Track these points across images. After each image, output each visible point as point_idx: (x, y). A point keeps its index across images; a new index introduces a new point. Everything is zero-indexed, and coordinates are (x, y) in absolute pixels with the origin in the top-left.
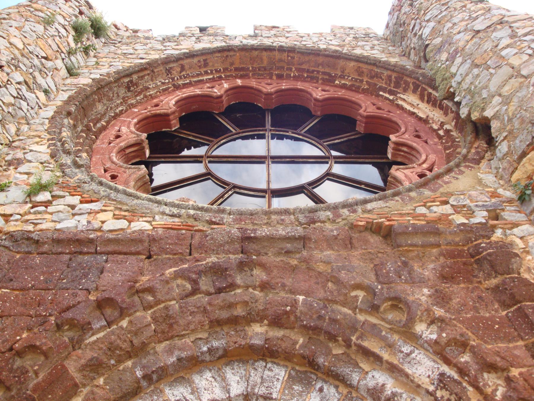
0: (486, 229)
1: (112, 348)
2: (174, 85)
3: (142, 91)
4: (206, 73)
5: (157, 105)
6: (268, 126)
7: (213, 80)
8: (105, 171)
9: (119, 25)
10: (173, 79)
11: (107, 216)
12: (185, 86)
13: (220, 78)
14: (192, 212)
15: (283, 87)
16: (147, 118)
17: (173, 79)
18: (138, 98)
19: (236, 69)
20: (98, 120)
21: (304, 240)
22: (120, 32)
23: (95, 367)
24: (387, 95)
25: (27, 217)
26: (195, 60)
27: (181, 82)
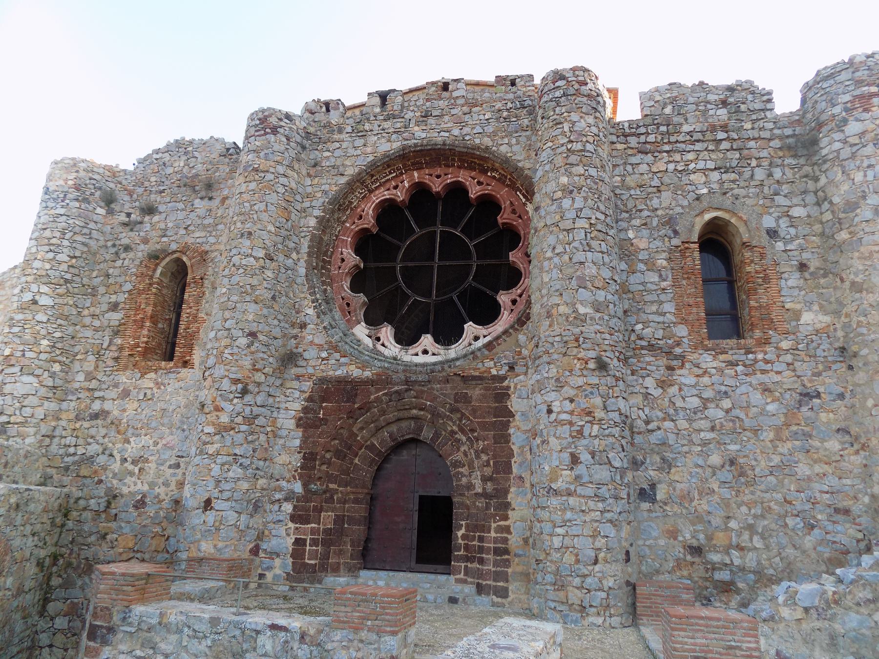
0: (503, 378)
1: (366, 423)
2: (369, 191)
3: (348, 206)
4: (390, 173)
5: (361, 217)
6: (438, 222)
7: (397, 176)
8: (343, 299)
9: (313, 106)
10: (367, 186)
11: (353, 367)
12: (376, 188)
13: (402, 174)
14: (386, 365)
15: (448, 181)
16: (357, 232)
17: (367, 186)
18: (347, 213)
19: (413, 164)
20: (328, 250)
21: (429, 381)
22: (317, 117)
23: (362, 429)
24: (521, 197)
25: (322, 367)
26: (380, 168)
27: (373, 187)
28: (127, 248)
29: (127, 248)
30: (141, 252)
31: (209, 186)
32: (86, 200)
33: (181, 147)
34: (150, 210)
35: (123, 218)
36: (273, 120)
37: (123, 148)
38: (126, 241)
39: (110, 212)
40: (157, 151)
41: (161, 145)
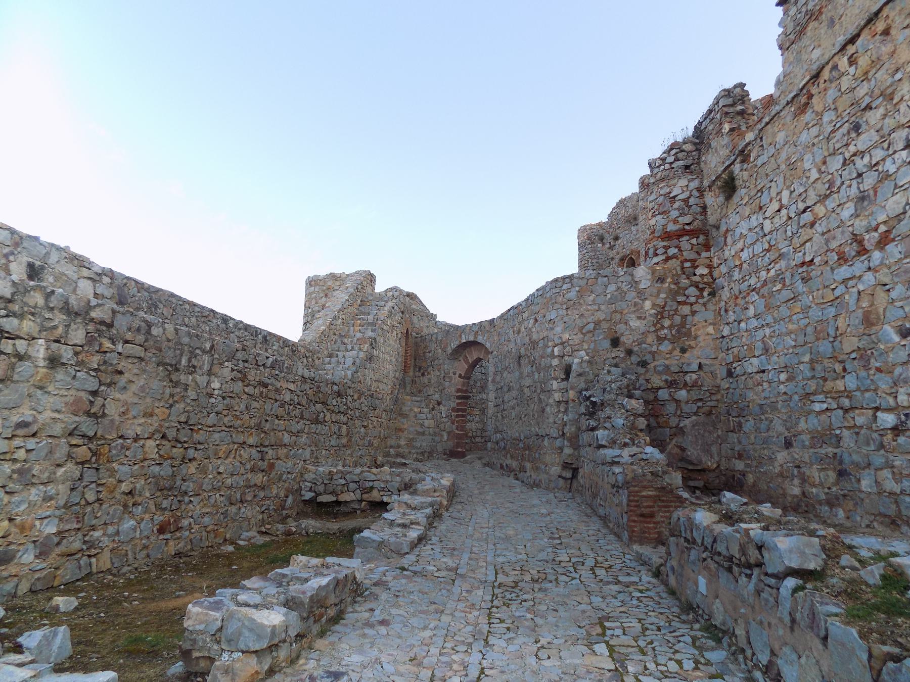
28: (612, 259)
29: (612, 259)
30: (618, 257)
31: (635, 219)
32: (593, 243)
33: (622, 203)
34: (616, 238)
35: (608, 246)
36: (646, 181)
37: (600, 214)
38: (611, 256)
39: (603, 244)
40: (614, 209)
41: (614, 205)
